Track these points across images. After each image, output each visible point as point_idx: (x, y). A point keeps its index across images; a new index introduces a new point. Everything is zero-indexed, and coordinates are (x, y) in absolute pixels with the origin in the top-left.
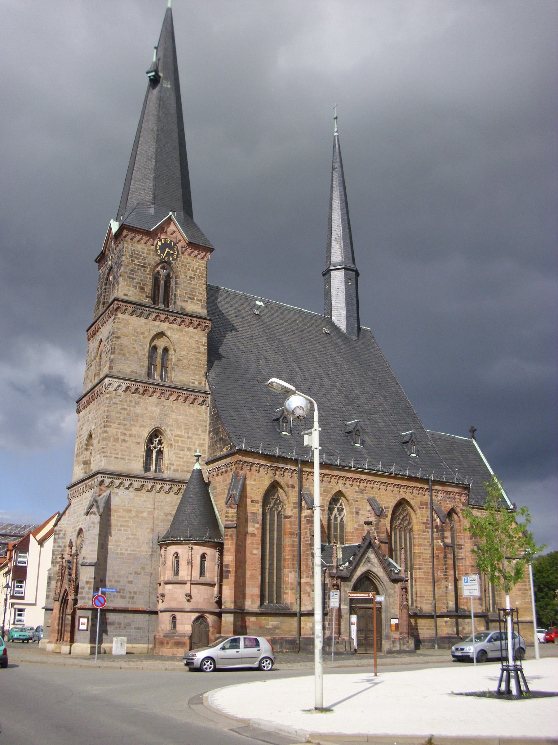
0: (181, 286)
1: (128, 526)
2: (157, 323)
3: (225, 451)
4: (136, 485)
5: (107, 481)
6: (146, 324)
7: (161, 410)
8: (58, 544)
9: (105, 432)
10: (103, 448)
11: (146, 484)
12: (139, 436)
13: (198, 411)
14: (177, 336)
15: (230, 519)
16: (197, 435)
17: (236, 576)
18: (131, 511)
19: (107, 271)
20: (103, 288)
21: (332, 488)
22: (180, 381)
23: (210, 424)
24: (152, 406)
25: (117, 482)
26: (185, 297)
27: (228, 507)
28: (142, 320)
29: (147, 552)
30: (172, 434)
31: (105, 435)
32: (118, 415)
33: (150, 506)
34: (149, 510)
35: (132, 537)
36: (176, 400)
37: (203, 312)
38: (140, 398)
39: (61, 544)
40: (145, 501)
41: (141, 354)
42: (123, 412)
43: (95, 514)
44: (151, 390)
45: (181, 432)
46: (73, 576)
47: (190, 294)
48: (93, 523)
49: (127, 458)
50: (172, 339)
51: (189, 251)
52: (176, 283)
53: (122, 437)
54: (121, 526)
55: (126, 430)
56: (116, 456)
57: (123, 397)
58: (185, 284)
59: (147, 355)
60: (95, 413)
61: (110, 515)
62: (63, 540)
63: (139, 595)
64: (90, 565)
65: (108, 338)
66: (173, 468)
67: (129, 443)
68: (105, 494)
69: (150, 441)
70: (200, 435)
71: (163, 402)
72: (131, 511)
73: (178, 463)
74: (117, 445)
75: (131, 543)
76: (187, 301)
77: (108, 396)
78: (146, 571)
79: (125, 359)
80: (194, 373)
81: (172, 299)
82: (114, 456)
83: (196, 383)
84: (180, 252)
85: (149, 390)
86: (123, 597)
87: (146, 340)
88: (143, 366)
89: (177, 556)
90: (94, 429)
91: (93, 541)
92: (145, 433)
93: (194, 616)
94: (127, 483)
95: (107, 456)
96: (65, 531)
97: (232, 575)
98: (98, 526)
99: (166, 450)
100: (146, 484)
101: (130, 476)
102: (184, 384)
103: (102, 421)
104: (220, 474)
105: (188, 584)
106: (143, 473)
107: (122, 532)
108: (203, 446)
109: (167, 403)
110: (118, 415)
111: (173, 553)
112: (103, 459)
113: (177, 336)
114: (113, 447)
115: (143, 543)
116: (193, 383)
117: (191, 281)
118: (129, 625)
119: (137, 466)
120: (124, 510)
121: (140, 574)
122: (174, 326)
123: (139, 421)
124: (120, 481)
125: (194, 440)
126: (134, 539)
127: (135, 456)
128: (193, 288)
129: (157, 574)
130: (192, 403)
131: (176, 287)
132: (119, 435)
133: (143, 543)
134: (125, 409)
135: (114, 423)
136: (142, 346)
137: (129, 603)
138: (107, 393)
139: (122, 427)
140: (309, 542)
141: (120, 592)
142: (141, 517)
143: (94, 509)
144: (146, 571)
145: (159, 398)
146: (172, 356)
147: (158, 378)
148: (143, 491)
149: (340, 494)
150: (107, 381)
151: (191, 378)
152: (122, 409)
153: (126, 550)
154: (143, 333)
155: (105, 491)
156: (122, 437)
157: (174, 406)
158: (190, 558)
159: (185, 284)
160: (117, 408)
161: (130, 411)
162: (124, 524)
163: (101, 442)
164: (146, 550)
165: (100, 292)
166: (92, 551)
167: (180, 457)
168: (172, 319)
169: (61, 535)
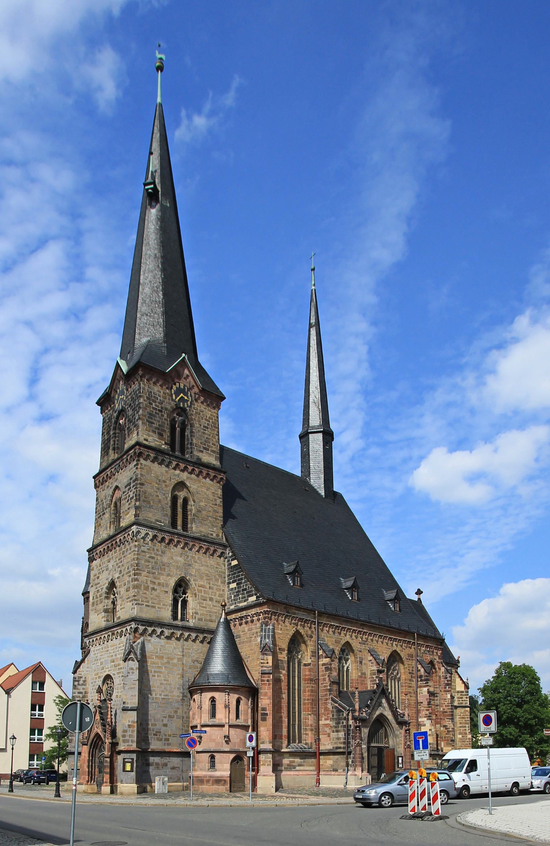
0: (197, 435)
1: (159, 672)
2: (177, 472)
4: (167, 632)
5: (141, 628)
6: (167, 472)
7: (185, 560)
9: (136, 580)
10: (134, 596)
11: (175, 631)
12: (167, 585)
13: (217, 562)
14: (195, 487)
16: (217, 585)
17: (273, 719)
18: (162, 657)
19: (115, 415)
20: (112, 433)
21: (341, 639)
22: (201, 532)
23: (229, 575)
24: (177, 556)
25: (150, 629)
26: (200, 447)
27: (263, 654)
28: (164, 468)
29: (178, 696)
30: (196, 584)
31: (136, 583)
32: (147, 564)
33: (179, 653)
34: (179, 657)
35: (165, 682)
36: (198, 551)
37: (217, 463)
38: (166, 547)
40: (175, 648)
41: (164, 502)
42: (151, 560)
43: (133, 660)
44: (176, 540)
45: (204, 582)
46: (109, 720)
47: (205, 445)
48: (132, 669)
49: (157, 606)
50: (191, 489)
51: (202, 399)
52: (192, 432)
53: (151, 586)
54: (155, 672)
55: (155, 578)
56: (147, 604)
57: (150, 545)
58: (200, 434)
59: (170, 504)
60: (118, 562)
61: (146, 662)
63: (173, 737)
64: (132, 710)
65: (129, 484)
66: (197, 616)
67: (158, 591)
68: (139, 641)
69: (175, 591)
70: (219, 586)
71: (186, 552)
72: (162, 658)
73: (202, 612)
74: (147, 593)
75: (165, 688)
76: (202, 452)
77: (137, 543)
78: (178, 714)
79: (149, 507)
80: (212, 525)
81: (188, 448)
82: (145, 603)
83: (214, 535)
84: (193, 399)
85: (174, 541)
86: (160, 740)
87: (168, 489)
88: (167, 515)
89: (213, 700)
90: (118, 578)
91: (133, 686)
92: (172, 583)
93: (232, 756)
94: (159, 630)
95: (139, 604)
97: (270, 719)
98: (137, 672)
99: (190, 599)
100: (175, 631)
101: (161, 625)
102: (204, 536)
103: (131, 569)
104: (244, 623)
105: (227, 727)
106: (172, 621)
107: (156, 677)
108: (223, 597)
109: (190, 554)
110: (147, 564)
112: (136, 606)
113: (195, 487)
114: (144, 595)
115: (175, 688)
116: (212, 535)
117: (205, 430)
118: (166, 765)
119: (166, 614)
120: (157, 657)
121: (173, 717)
122: (193, 476)
123: (166, 570)
124: (153, 629)
125: (214, 591)
126: (166, 684)
127: (164, 605)
128: (207, 438)
129: (188, 717)
130: (212, 555)
131: (191, 436)
132: (149, 582)
133: (175, 688)
134: (153, 558)
135: (144, 571)
136: (164, 494)
137: (165, 744)
138: (136, 541)
139: (151, 575)
141: (157, 735)
142: (172, 663)
143: (132, 656)
144: (178, 714)
145: (183, 548)
146: (192, 507)
147: (179, 527)
148: (173, 639)
149: (347, 644)
150: (134, 528)
151: (210, 529)
152: (150, 557)
153: (161, 695)
154: (164, 482)
155: (139, 638)
156: (151, 586)
157: (197, 557)
158: (227, 702)
159: (200, 434)
160: (145, 556)
161: (157, 559)
162: (157, 670)
163: (131, 590)
164: (177, 694)
165: (106, 437)
166: (132, 696)
167: (203, 607)
168: (190, 468)
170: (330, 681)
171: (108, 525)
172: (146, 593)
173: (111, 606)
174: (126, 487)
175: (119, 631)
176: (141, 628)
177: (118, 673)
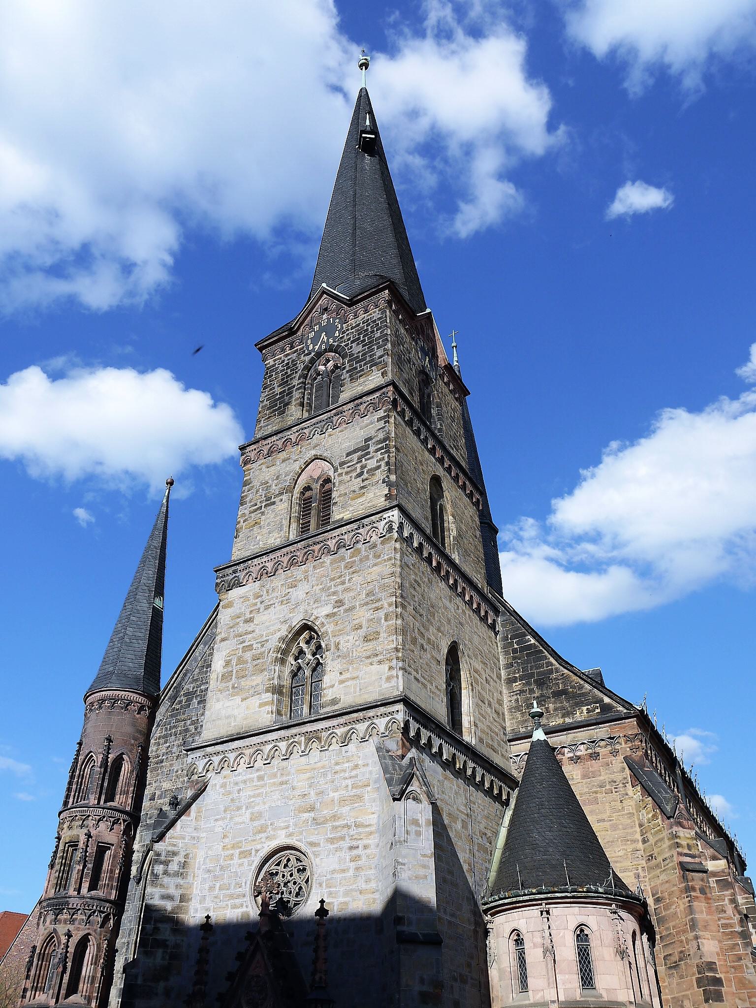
3: (582, 714)
8: (163, 891)
15: (686, 851)
23: (509, 666)
39: (172, 891)
62: (179, 880)
89: (582, 935)
91: (422, 872)
96: (186, 856)
111: (573, 925)
140: (738, 929)
169: (173, 867)
170: (740, 913)
171: (285, 523)
172: (413, 651)
173: (287, 682)
174: (348, 455)
175: (340, 731)
176: (414, 726)
177: (332, 841)
